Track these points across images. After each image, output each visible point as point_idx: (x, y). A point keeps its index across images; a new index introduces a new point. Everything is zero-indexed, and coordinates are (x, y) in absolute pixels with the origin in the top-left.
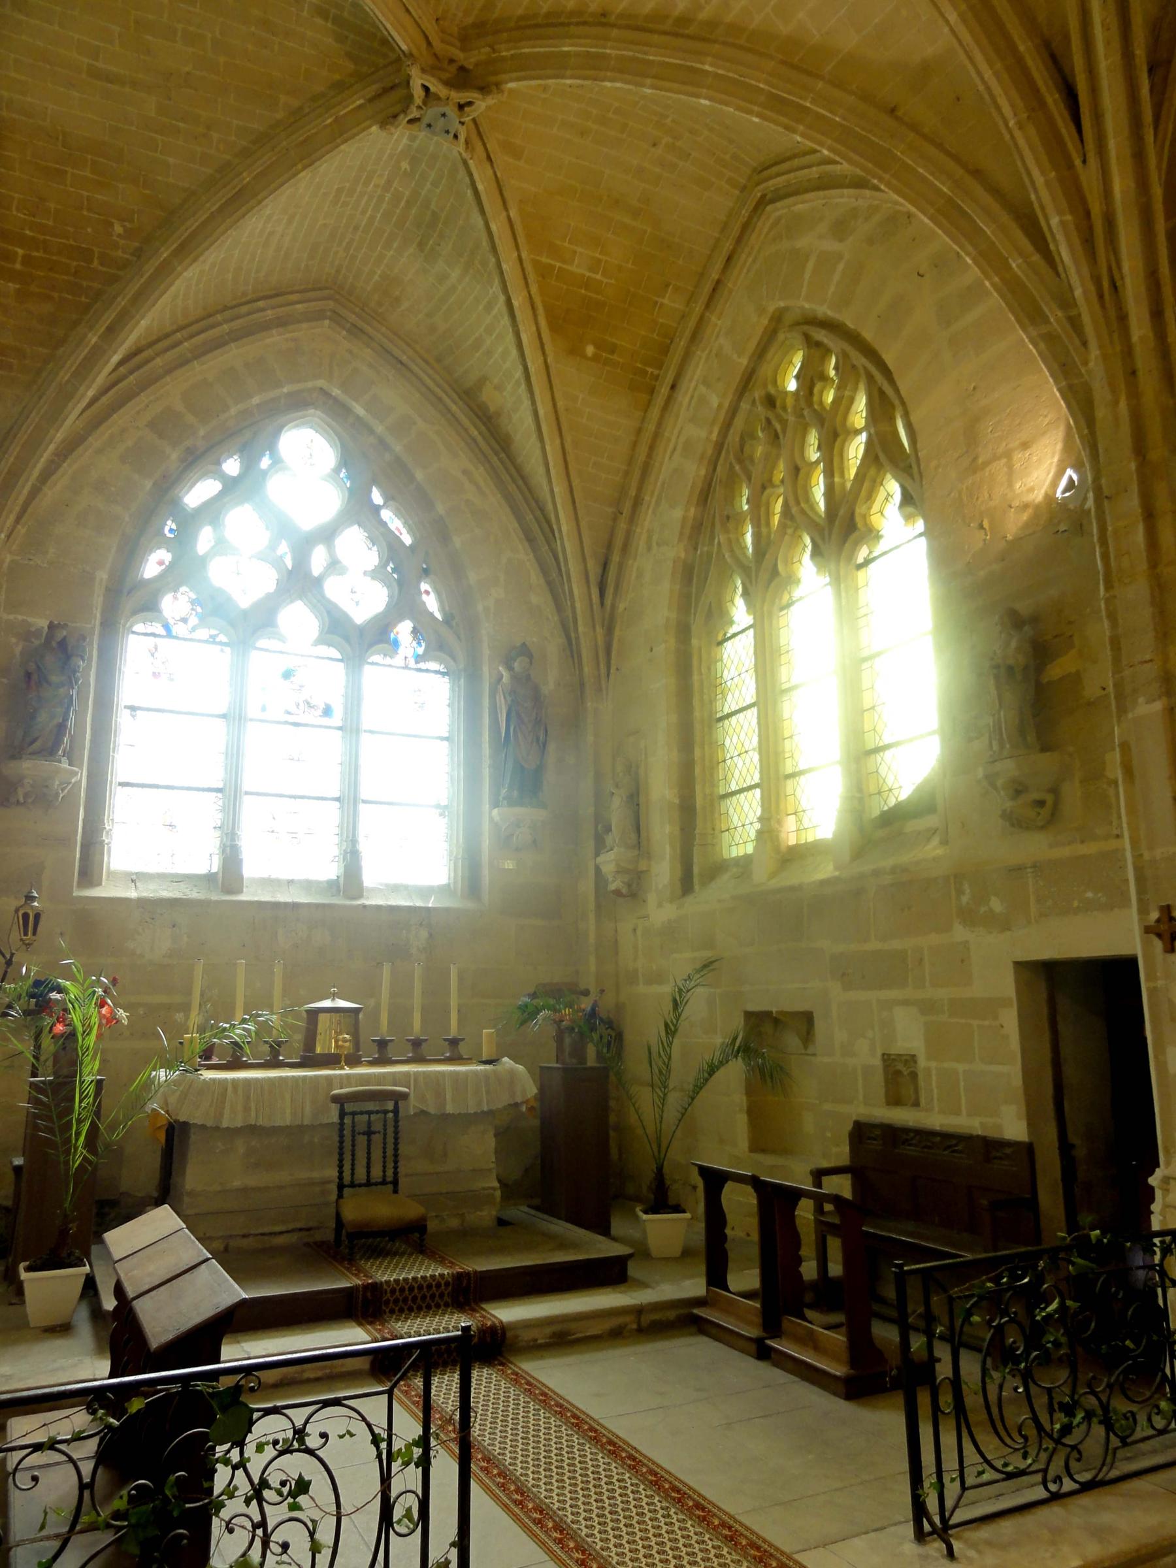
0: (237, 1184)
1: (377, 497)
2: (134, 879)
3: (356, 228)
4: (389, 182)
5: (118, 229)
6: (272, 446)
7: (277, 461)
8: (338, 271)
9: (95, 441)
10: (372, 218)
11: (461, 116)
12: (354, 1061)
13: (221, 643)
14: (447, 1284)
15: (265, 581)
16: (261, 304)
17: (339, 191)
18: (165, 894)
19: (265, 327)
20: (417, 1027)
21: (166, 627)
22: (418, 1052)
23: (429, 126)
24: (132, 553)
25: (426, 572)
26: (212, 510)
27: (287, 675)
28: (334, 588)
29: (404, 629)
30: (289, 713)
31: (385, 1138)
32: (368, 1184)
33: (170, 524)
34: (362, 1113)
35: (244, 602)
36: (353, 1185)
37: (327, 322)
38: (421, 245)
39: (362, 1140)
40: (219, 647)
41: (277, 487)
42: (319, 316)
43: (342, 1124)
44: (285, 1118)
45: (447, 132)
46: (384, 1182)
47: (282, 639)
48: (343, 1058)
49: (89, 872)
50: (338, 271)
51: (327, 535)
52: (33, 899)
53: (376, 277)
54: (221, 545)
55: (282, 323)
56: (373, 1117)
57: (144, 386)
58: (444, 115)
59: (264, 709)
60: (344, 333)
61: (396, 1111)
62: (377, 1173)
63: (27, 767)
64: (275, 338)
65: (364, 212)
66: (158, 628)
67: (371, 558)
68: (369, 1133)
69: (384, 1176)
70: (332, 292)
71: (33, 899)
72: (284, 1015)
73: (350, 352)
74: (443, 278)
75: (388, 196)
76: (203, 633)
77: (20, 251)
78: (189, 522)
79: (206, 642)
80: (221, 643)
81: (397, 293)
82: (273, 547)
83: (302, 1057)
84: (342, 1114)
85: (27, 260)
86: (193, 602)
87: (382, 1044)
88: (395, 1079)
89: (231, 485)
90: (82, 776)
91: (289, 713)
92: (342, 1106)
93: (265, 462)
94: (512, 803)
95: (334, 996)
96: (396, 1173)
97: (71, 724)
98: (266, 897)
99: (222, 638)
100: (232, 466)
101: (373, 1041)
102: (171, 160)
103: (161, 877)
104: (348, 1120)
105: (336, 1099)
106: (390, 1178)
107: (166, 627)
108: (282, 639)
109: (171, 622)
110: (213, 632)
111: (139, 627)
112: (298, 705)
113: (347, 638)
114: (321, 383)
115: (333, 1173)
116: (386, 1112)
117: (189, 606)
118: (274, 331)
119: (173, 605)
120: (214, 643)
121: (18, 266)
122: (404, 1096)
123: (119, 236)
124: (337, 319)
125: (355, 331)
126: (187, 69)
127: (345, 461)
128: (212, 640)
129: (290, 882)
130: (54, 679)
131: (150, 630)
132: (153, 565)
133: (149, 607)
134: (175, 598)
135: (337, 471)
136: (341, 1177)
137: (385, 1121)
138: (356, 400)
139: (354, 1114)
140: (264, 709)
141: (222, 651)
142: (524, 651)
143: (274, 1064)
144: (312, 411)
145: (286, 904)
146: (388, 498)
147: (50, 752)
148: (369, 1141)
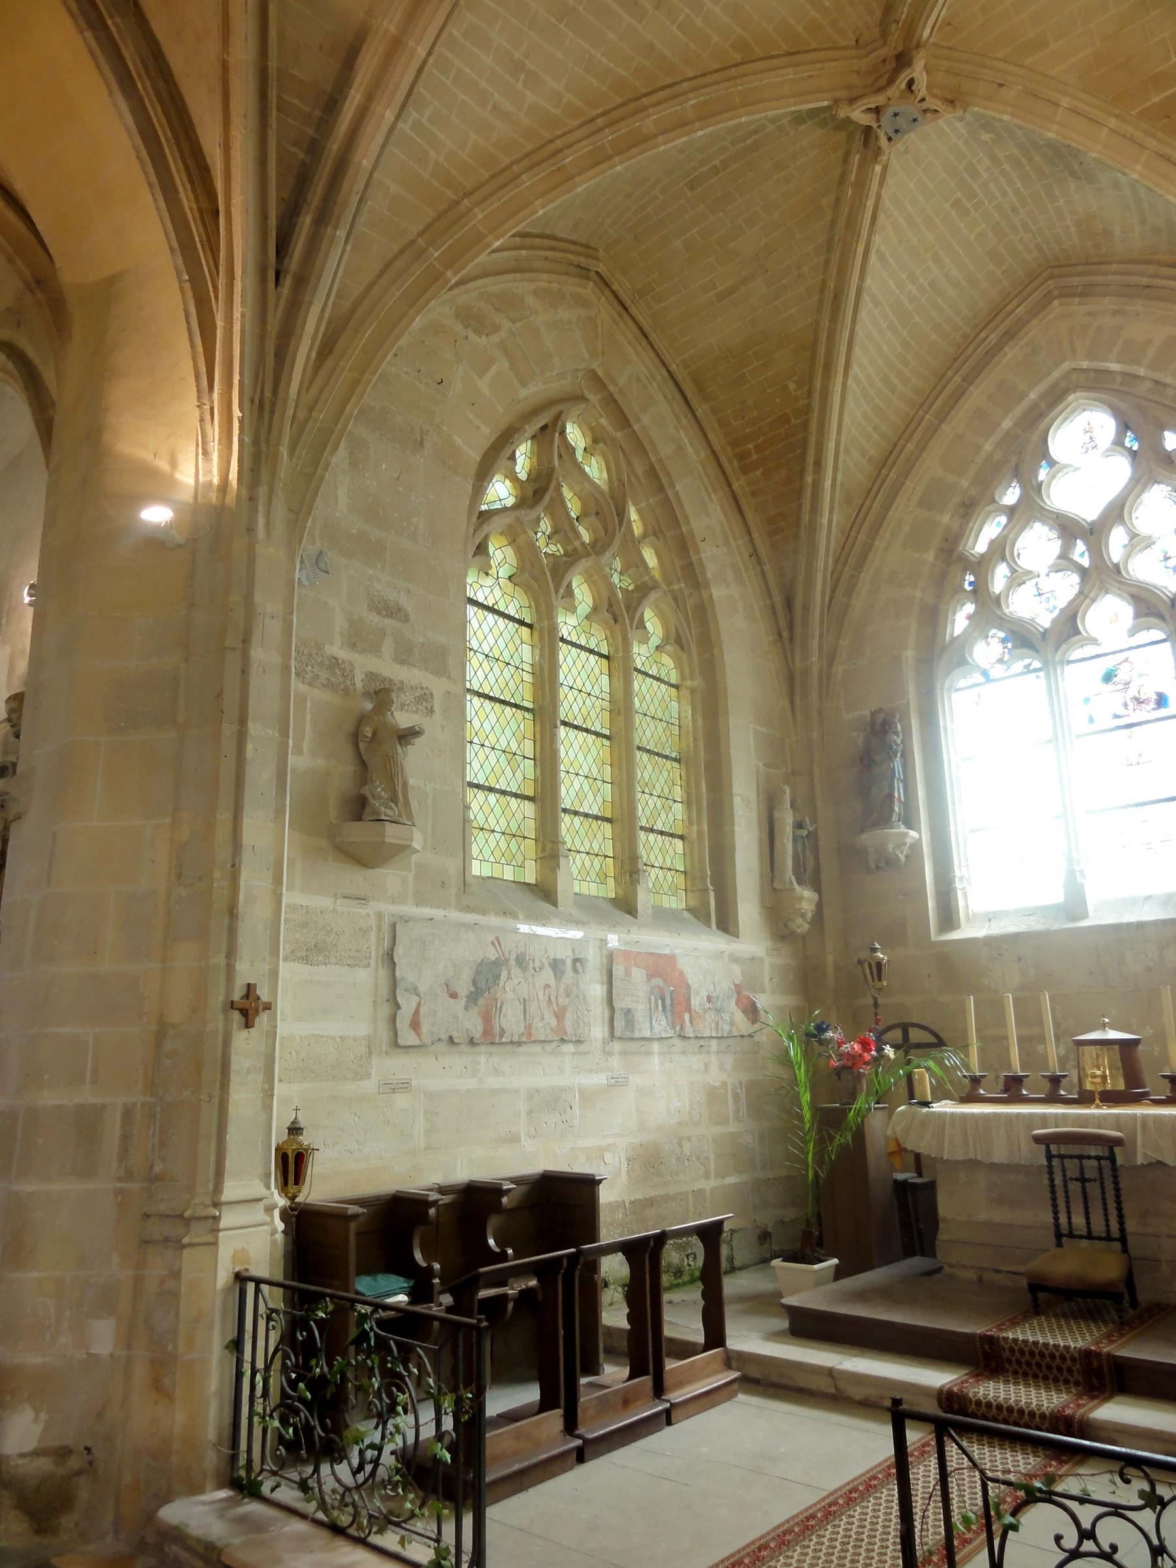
0: (983, 1217)
2: (990, 918)
3: (1014, 209)
4: (993, 158)
5: (792, 386)
6: (1043, 452)
7: (1052, 463)
8: (1041, 250)
9: (880, 544)
10: (1017, 192)
11: (916, 97)
12: (1136, 1099)
13: (1036, 670)
14: (1073, 1359)
16: (983, 335)
17: (957, 204)
18: (1012, 929)
19: (998, 348)
21: (985, 673)
23: (897, 131)
26: (1001, 549)
27: (1108, 677)
30: (1116, 716)
31: (1103, 1188)
32: (1090, 1236)
33: (970, 578)
34: (1071, 1157)
35: (1045, 621)
36: (1071, 1235)
37: (1056, 303)
38: (1073, 174)
39: (1075, 1187)
40: (1033, 675)
42: (1046, 301)
43: (1050, 1167)
44: (1000, 1155)
45: (915, 120)
46: (1108, 1238)
47: (1094, 641)
48: (1097, 1096)
49: (948, 919)
50: (1041, 250)
51: (1117, 512)
52: (875, 950)
53: (1073, 229)
54: (1018, 578)
55: (1010, 336)
56: (1086, 1162)
57: (906, 474)
58: (896, 115)
59: (1091, 720)
60: (1077, 300)
61: (1112, 1159)
62: (1098, 1227)
63: (868, 839)
64: (1011, 353)
65: (1005, 194)
66: (977, 677)
68: (1083, 1180)
69: (1108, 1231)
70: (1049, 271)
71: (875, 950)
73: (1089, 314)
74: (1116, 185)
75: (1007, 166)
76: (1018, 666)
77: (750, 446)
78: (982, 566)
79: (1022, 673)
80: (1036, 670)
81: (1101, 227)
82: (1064, 556)
83: (1079, 1093)
84: (1049, 1157)
85: (758, 449)
86: (1003, 641)
88: (1117, 1122)
90: (921, 835)
91: (1116, 716)
92: (1048, 1147)
93: (1043, 474)
95: (1103, 1026)
96: (1122, 1230)
97: (899, 792)
98: (1110, 919)
99: (1037, 664)
100: (1011, 495)
101: (1163, 1076)
102: (793, 311)
103: (1017, 913)
104: (1055, 1162)
105: (1038, 1139)
106: (1115, 1233)
107: (985, 673)
108: (1094, 641)
109: (988, 667)
110: (1027, 661)
111: (962, 683)
112: (1126, 705)
113: (1161, 617)
114: (1066, 366)
115: (1048, 1217)
116: (1098, 1158)
117: (1000, 646)
118: (1006, 349)
120: (1030, 672)
121: (755, 457)
122: (1118, 1142)
123: (795, 391)
124: (1067, 293)
125: (1087, 292)
126: (763, 242)
127: (1124, 426)
128: (1028, 670)
129: (1149, 898)
130: (877, 758)
131: (970, 682)
132: (961, 619)
133: (962, 661)
134: (988, 644)
135: (1119, 442)
136: (1057, 1225)
137: (1100, 1169)
138: (1106, 360)
139: (1062, 1157)
140: (1091, 720)
141: (1038, 677)
143: (1053, 1098)
144: (1071, 397)
145: (1129, 926)
148: (1084, 1189)
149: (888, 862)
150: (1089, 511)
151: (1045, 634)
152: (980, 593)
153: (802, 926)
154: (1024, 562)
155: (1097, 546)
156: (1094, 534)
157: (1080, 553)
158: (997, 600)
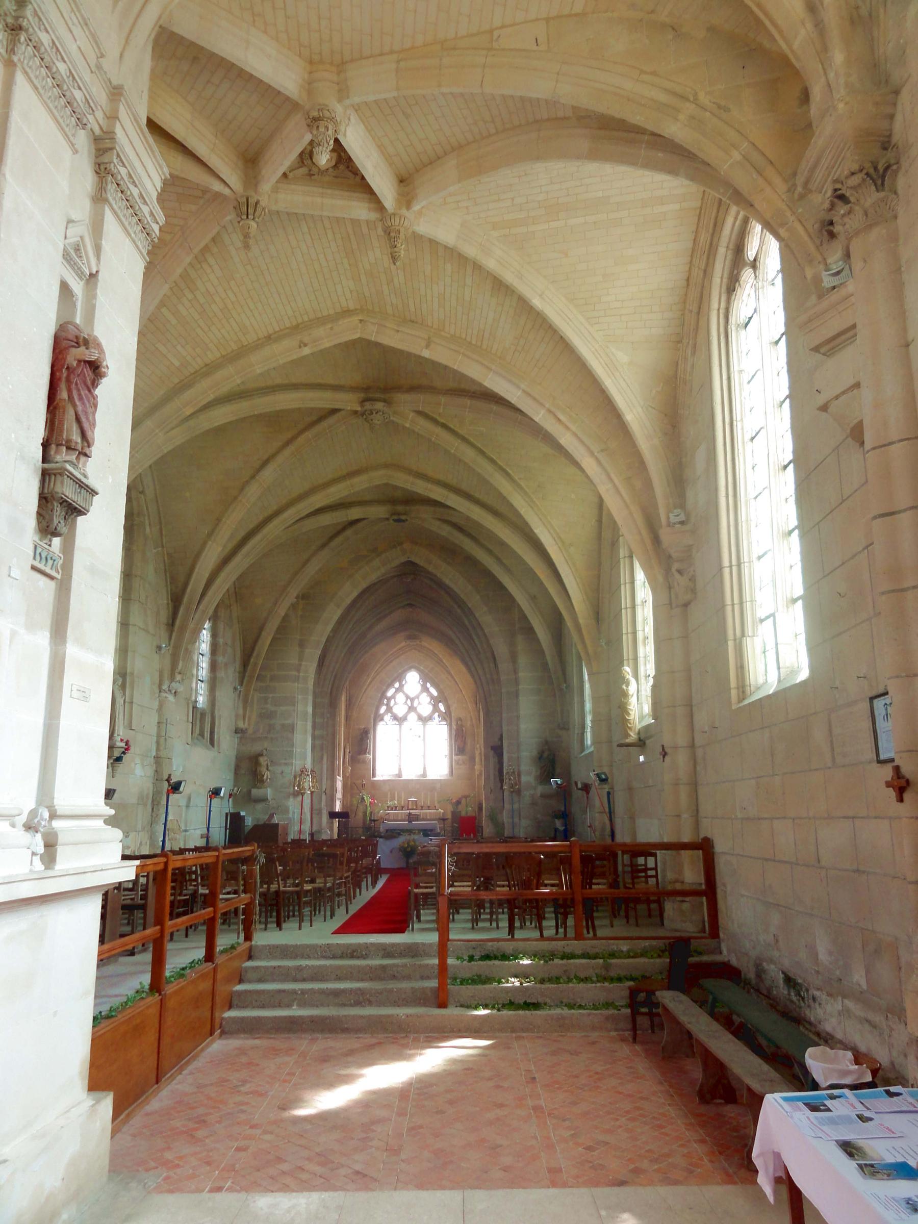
1: (428, 685)
15: (406, 709)
20: (429, 804)
22: (429, 808)
24: (378, 708)
25: (440, 702)
26: (393, 697)
28: (420, 710)
29: (436, 715)
33: (385, 700)
41: (406, 689)
49: (374, 775)
51: (417, 697)
54: (395, 703)
63: (361, 757)
67: (428, 699)
72: (398, 801)
78: (389, 699)
87: (422, 807)
89: (398, 690)
93: (404, 682)
94: (456, 755)
100: (397, 685)
119: (387, 717)
125: (419, 651)
132: (383, 709)
142: (460, 719)
146: (431, 685)
147: (365, 753)
149: (364, 762)
150: (412, 695)
151: (401, 718)
152: (388, 705)
153: (348, 775)
154: (397, 701)
155: (412, 700)
156: (412, 700)
157: (409, 702)
158: (392, 708)
